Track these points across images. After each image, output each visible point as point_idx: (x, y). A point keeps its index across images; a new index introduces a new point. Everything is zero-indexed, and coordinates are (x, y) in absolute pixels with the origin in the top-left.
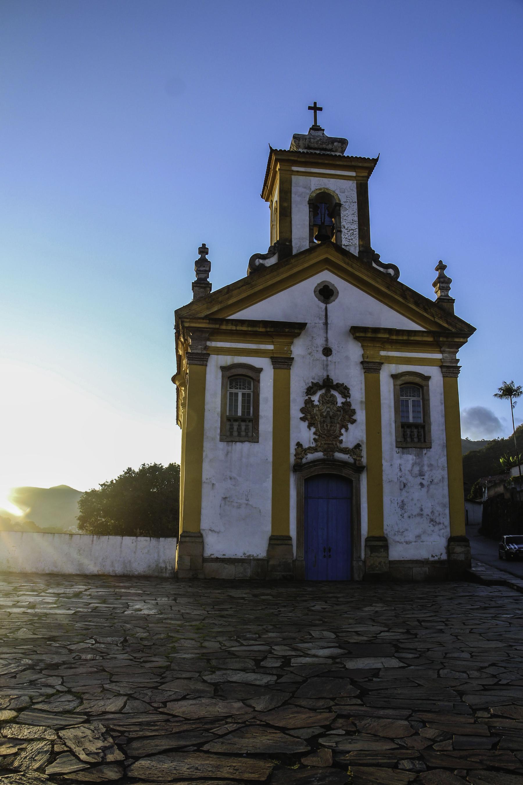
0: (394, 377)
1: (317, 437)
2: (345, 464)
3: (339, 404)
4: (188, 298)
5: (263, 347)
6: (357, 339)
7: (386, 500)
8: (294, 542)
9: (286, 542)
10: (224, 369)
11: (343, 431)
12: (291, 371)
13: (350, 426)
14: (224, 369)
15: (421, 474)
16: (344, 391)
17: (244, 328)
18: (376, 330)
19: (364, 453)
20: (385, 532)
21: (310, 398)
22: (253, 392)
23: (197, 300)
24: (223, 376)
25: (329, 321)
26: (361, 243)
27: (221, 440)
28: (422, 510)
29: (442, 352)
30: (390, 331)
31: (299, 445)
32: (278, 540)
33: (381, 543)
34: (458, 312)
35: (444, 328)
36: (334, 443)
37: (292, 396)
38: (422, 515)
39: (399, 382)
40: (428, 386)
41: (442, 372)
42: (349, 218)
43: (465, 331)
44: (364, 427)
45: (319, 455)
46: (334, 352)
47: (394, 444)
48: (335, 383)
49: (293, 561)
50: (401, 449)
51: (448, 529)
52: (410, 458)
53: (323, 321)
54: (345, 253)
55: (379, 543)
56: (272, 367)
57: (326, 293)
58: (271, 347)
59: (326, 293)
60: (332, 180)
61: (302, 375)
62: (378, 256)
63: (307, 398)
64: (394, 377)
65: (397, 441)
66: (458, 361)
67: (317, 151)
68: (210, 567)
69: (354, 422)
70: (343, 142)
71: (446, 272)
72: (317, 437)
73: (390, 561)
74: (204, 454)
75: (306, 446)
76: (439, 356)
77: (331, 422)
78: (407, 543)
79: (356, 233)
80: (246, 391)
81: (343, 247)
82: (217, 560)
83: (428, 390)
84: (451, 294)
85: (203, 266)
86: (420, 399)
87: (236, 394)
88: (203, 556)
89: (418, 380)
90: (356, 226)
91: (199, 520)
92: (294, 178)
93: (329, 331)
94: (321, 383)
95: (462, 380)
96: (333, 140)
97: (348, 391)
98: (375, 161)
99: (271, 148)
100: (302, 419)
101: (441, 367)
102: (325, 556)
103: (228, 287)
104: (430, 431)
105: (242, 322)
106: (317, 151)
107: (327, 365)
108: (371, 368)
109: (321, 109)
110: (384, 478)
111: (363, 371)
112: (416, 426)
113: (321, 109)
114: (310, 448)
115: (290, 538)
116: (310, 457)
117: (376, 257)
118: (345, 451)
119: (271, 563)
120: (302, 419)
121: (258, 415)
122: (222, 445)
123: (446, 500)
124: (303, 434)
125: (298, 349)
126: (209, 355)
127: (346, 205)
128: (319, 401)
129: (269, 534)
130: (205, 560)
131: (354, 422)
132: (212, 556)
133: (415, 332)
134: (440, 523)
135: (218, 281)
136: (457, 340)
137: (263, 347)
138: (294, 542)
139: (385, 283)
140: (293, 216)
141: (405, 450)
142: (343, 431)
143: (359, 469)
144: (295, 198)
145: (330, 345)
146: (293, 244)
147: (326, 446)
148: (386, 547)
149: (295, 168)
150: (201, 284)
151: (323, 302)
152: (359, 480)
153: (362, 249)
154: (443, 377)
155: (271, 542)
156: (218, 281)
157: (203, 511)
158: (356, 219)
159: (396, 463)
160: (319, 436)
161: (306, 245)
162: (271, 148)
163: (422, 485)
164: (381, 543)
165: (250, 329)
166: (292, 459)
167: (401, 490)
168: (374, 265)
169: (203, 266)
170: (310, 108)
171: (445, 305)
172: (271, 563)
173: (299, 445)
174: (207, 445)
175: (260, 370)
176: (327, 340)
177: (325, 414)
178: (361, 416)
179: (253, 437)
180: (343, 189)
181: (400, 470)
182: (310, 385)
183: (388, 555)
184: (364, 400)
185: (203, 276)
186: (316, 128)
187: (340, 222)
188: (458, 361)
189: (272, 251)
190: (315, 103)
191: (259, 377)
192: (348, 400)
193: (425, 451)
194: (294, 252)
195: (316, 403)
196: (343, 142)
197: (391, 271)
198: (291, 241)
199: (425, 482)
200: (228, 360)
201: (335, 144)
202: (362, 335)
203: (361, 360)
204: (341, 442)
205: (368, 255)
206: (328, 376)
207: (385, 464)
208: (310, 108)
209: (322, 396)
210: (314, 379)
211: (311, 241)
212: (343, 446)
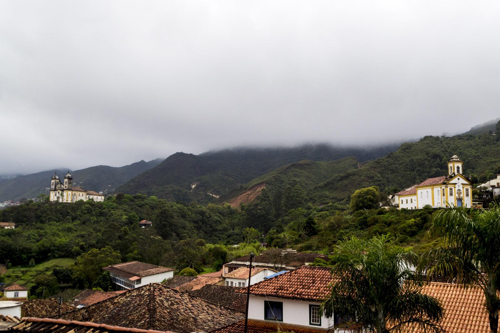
16: (461, 191)
52: (467, 198)
57: (459, 179)
59: (459, 179)
61: (457, 189)
108: (463, 188)
124: (457, 195)
125: (456, 186)
200: (450, 187)
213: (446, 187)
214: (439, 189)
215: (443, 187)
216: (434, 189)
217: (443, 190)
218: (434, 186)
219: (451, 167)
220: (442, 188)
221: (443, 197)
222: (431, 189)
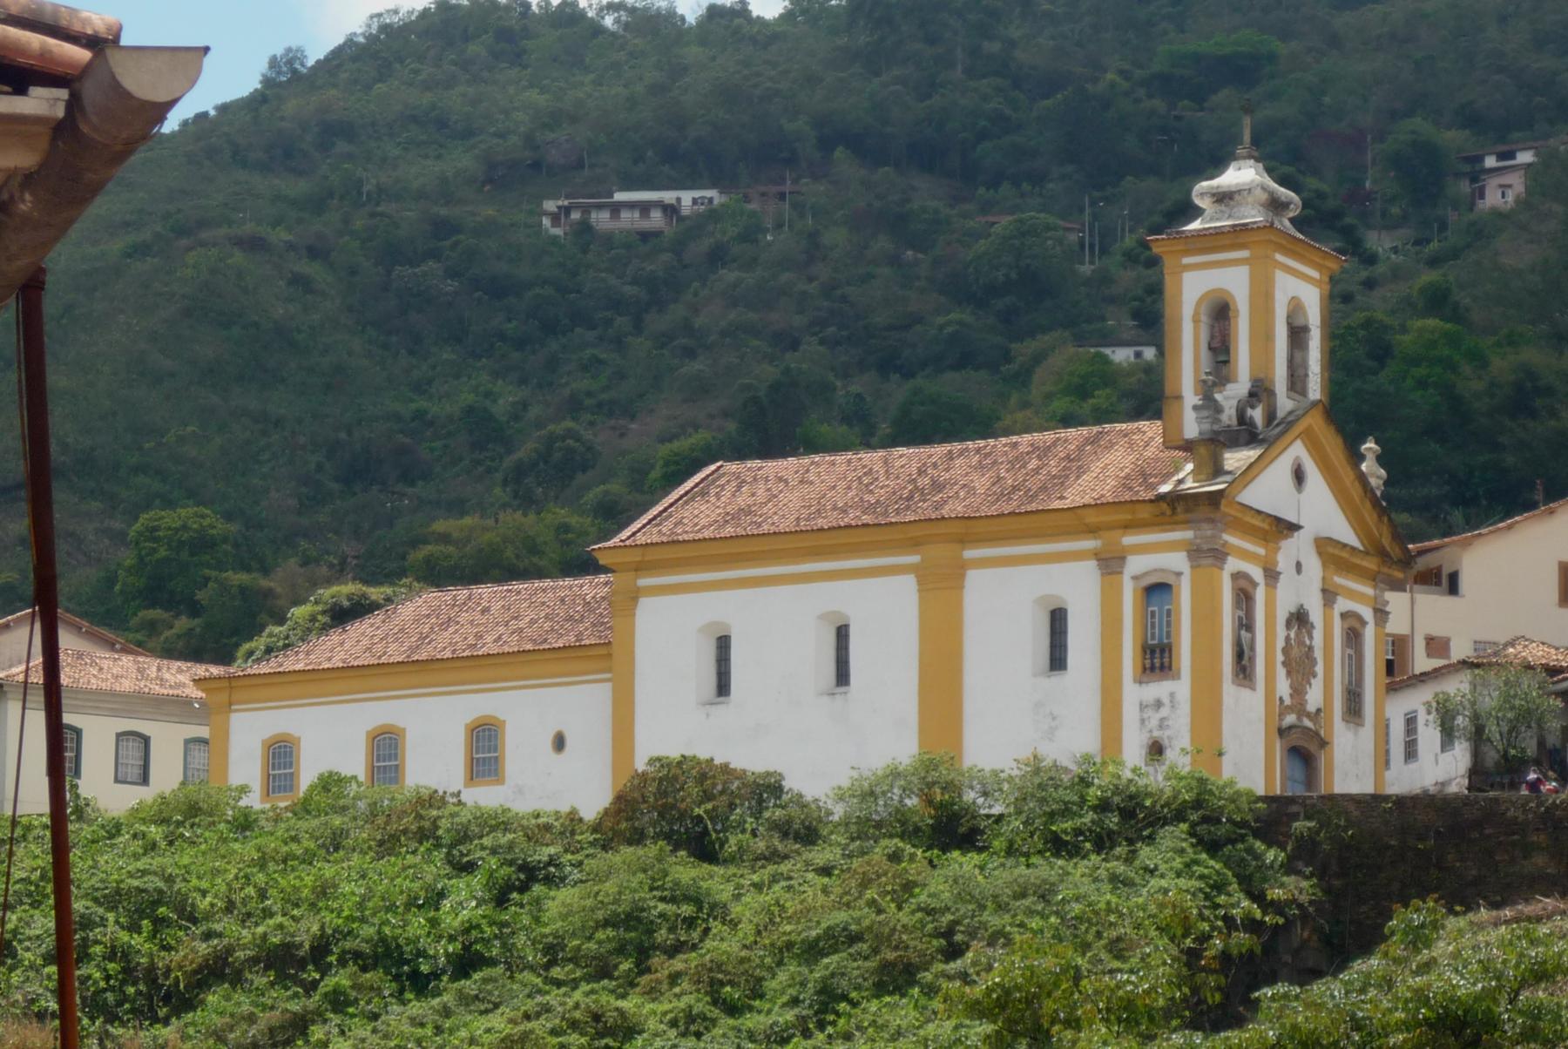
6: (1320, 554)
18: (1345, 545)
29: (1375, 587)
57: (1299, 476)
59: (1299, 476)
64: (1344, 616)
89: (1357, 625)
108: (1329, 595)
118: (1308, 715)
124: (1283, 687)
131: (1315, 676)
175: (1255, 585)
202: (1331, 550)
213: (1196, 553)
214: (1075, 583)
215: (1159, 554)
216: (976, 580)
217: (1157, 590)
218: (964, 540)
219: (1220, 312)
220: (1137, 565)
221: (1134, 694)
222: (908, 583)
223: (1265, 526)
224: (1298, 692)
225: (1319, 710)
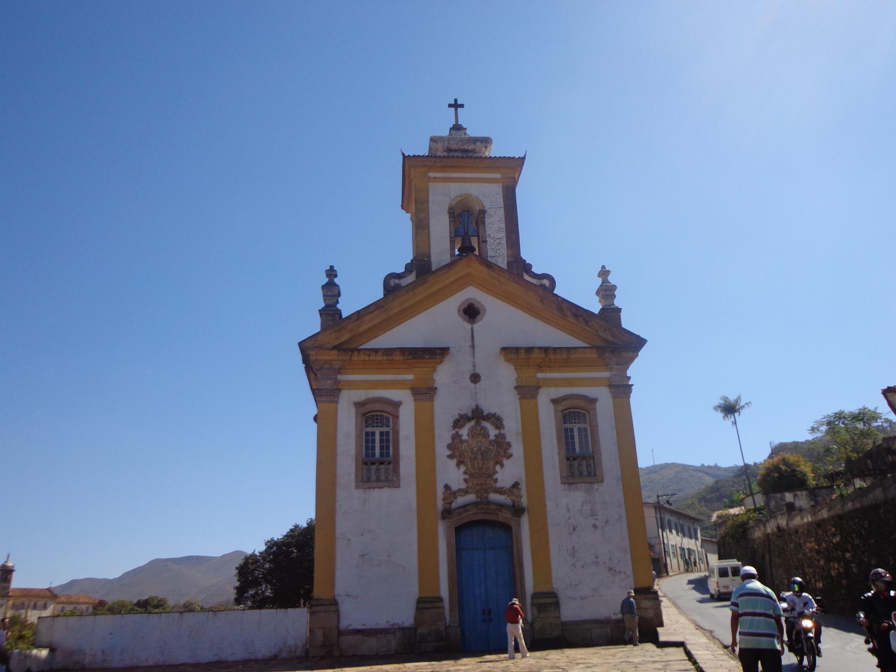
0: (555, 401)
1: (467, 477)
2: (501, 506)
3: (492, 437)
4: (313, 325)
5: (400, 377)
6: (508, 360)
7: (553, 547)
8: (446, 603)
9: (436, 605)
10: (358, 405)
11: (498, 468)
12: (435, 402)
13: (505, 462)
14: (358, 405)
15: (593, 514)
16: (497, 421)
17: (379, 358)
18: (529, 350)
19: (524, 492)
20: (555, 586)
21: (457, 432)
22: (393, 429)
23: (324, 327)
24: (357, 413)
25: (476, 343)
26: (510, 253)
27: (357, 487)
28: (597, 557)
29: (611, 370)
30: (546, 350)
31: (447, 487)
32: (426, 603)
33: (550, 600)
34: (628, 322)
35: (609, 341)
36: (488, 482)
37: (437, 432)
38: (597, 563)
39: (561, 408)
40: (595, 410)
41: (611, 392)
42: (495, 225)
43: (635, 343)
44: (522, 462)
45: (471, 497)
46: (483, 377)
47: (559, 479)
48: (485, 414)
49: (446, 628)
50: (567, 486)
51: (632, 579)
52: (577, 496)
53: (470, 343)
54: (489, 265)
55: (547, 601)
56: (412, 399)
57: (471, 312)
58: (410, 377)
59: (471, 312)
60: (475, 185)
61: (448, 405)
62: (530, 266)
63: (454, 432)
64: (555, 401)
65: (562, 477)
66: (629, 378)
67: (459, 152)
68: (346, 640)
69: (510, 456)
70: (486, 141)
71: (612, 279)
72: (467, 477)
73: (563, 623)
74: (338, 504)
75: (455, 488)
76: (606, 374)
77: (483, 459)
78: (582, 598)
79: (504, 241)
80: (385, 429)
81: (489, 259)
82: (358, 632)
83: (595, 415)
84: (617, 303)
85: (331, 290)
86: (587, 426)
87: (373, 434)
88: (338, 627)
89: (582, 404)
90: (503, 234)
91: (333, 584)
92: (432, 186)
93: (476, 355)
94: (470, 415)
95: (636, 400)
96: (475, 140)
97: (501, 422)
98: (522, 160)
99: (403, 154)
100: (450, 457)
101: (610, 386)
102: (484, 620)
103: (358, 312)
104: (601, 463)
105: (376, 351)
106: (459, 152)
107: (476, 394)
108: (527, 392)
109: (462, 106)
110: (549, 521)
111: (518, 397)
112: (584, 458)
113: (462, 106)
114: (459, 490)
115: (440, 600)
116: (460, 500)
117: (527, 268)
118: (500, 491)
119: (420, 631)
120: (448, 456)
121: (399, 456)
122: (357, 493)
123: (627, 543)
124: (451, 474)
125: (443, 375)
126: (340, 390)
127: (490, 212)
128: (468, 435)
129: (416, 596)
130: (340, 633)
131: (510, 456)
132: (350, 628)
133: (569, 349)
134: (620, 573)
135: (347, 307)
136: (625, 355)
137: (400, 377)
138: (446, 603)
139: (540, 295)
140: (431, 228)
141: (573, 486)
142: (498, 468)
143: (518, 511)
144: (433, 208)
145: (478, 371)
146: (433, 259)
147: (478, 487)
148: (557, 605)
149: (431, 175)
150: (330, 313)
151: (469, 322)
152: (519, 525)
153: (510, 260)
154: (613, 398)
155: (420, 606)
156: (347, 307)
157: (338, 573)
158: (503, 226)
159: (562, 502)
160: (470, 475)
161: (447, 259)
162: (403, 154)
163: (595, 526)
164: (550, 600)
165: (385, 358)
166: (440, 504)
167: (570, 534)
168: (526, 277)
169: (331, 290)
170: (450, 106)
171: (611, 314)
172: (420, 631)
173: (447, 487)
174: (341, 495)
175: (397, 405)
176: (474, 365)
177: (475, 449)
178: (517, 449)
179: (392, 479)
180: (488, 195)
181: (568, 510)
182: (457, 417)
183: (559, 613)
184: (520, 430)
185: (330, 302)
186: (457, 127)
187: (485, 231)
188: (629, 378)
189: (409, 268)
190: (456, 100)
191: (397, 411)
192: (502, 432)
193: (596, 486)
194: (434, 268)
195: (465, 437)
196: (486, 141)
197: (546, 282)
198: (429, 256)
199: (597, 523)
200: (361, 395)
201: (478, 144)
203: (515, 384)
204: (496, 480)
205: (519, 266)
206: (477, 406)
207: (550, 505)
208: (450, 106)
209: (471, 429)
210: (461, 410)
211: (453, 255)
212: (499, 485)
223: (398, 357)
224: (481, 476)
225: (516, 485)
